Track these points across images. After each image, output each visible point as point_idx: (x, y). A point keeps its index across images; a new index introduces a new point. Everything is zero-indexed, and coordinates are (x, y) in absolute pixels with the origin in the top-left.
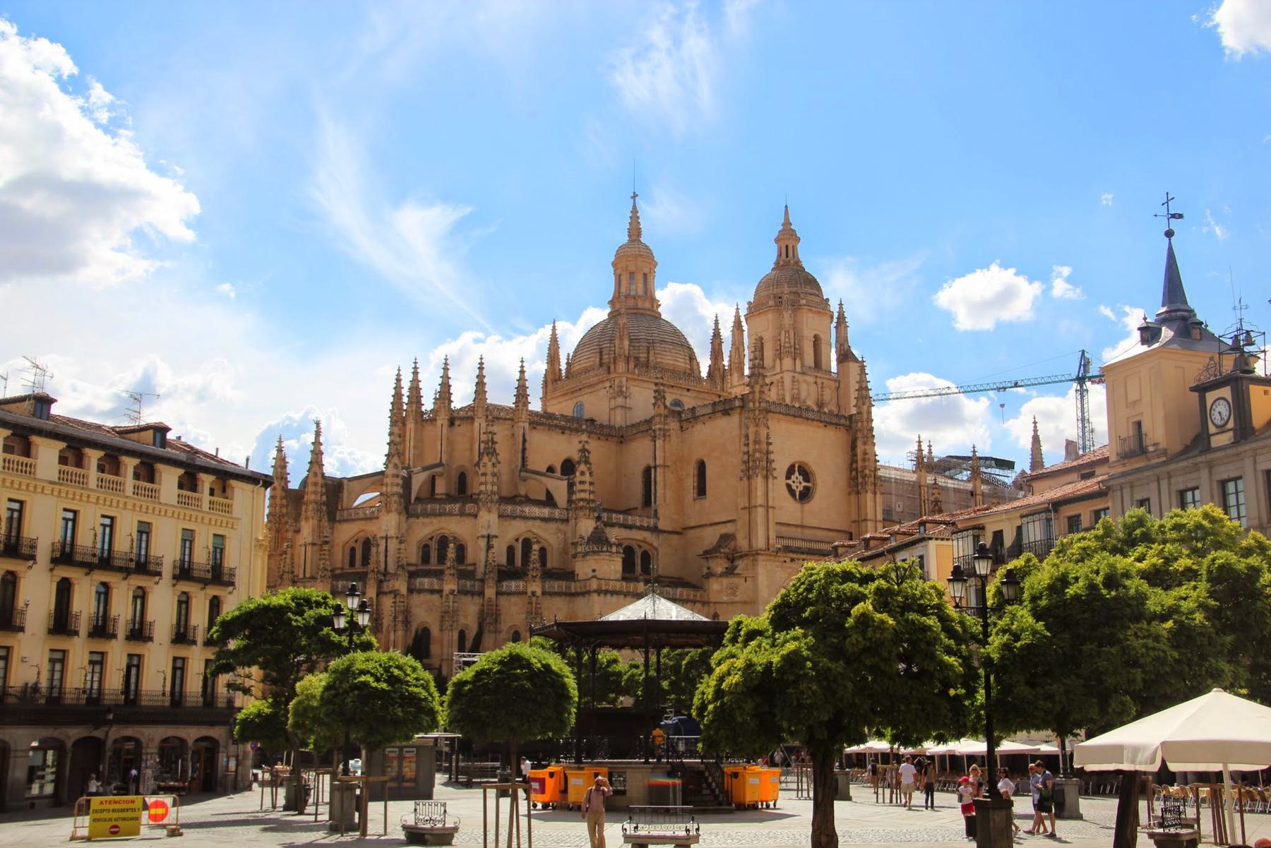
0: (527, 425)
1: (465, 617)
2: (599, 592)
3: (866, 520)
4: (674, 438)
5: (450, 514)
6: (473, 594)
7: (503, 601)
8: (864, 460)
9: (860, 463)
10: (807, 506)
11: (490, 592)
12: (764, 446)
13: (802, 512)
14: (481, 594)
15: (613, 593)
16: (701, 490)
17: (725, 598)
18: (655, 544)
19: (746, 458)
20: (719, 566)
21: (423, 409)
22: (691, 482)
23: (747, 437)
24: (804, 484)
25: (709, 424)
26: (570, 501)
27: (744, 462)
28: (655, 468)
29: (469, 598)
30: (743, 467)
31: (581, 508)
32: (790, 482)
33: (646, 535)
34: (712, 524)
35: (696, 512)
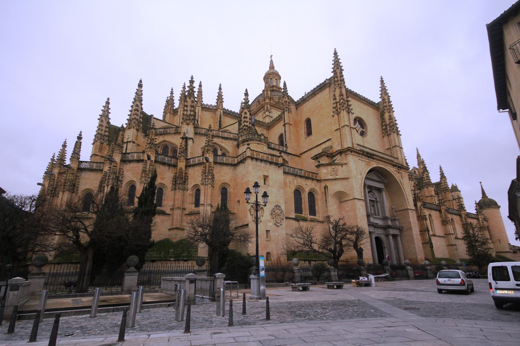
0: (222, 111)
1: (163, 179)
2: (252, 158)
3: (395, 146)
5: (169, 134)
6: (169, 165)
7: (191, 171)
8: (390, 119)
9: (388, 122)
11: (182, 165)
12: (345, 97)
13: (363, 141)
14: (175, 166)
15: (261, 161)
16: (309, 133)
17: (330, 177)
19: (335, 106)
20: (324, 160)
21: (175, 108)
22: (303, 131)
23: (334, 95)
25: (310, 101)
26: (239, 129)
27: (334, 108)
28: (284, 125)
30: (334, 110)
31: (245, 129)
34: (316, 147)
35: (306, 143)
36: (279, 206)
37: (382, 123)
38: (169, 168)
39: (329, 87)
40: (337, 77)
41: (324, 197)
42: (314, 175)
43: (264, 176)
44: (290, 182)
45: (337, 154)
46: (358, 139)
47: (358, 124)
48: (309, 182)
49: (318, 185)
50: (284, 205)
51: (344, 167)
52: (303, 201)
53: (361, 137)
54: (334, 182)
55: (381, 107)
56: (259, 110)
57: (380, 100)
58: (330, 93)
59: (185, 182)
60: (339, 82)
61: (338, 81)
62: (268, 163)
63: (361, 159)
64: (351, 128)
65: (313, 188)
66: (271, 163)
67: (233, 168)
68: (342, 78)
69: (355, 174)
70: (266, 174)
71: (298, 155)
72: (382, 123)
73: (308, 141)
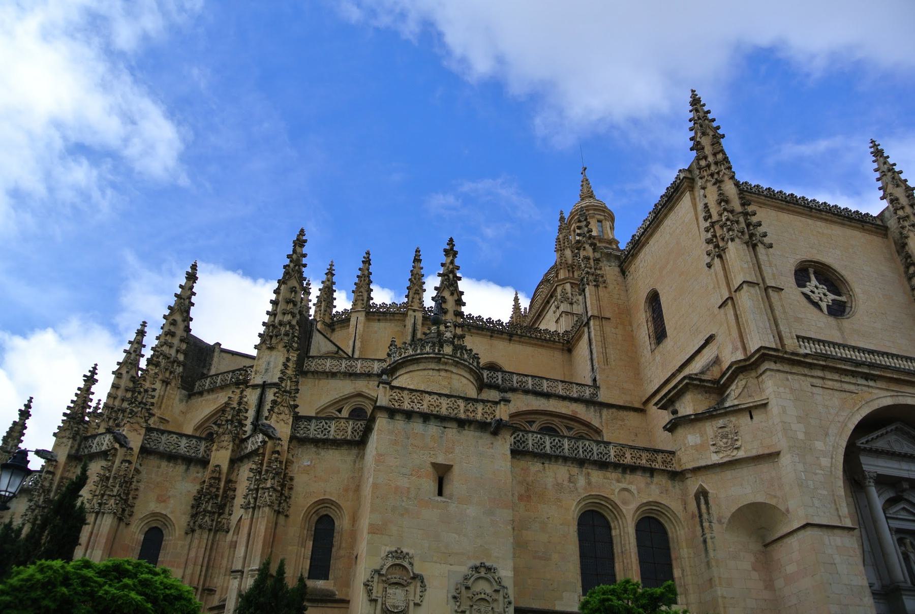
0: (419, 315)
1: (161, 499)
2: (392, 413)
4: (611, 287)
6: (188, 461)
10: (846, 323)
12: (736, 204)
13: (840, 329)
14: (204, 462)
15: (426, 417)
16: (660, 334)
17: (715, 459)
18: (596, 422)
19: (709, 235)
23: (706, 206)
24: (831, 297)
25: (652, 241)
27: (709, 242)
29: (181, 468)
30: (711, 247)
32: (806, 290)
33: (580, 411)
36: (488, 569)
37: (908, 268)
38: (187, 469)
39: (692, 189)
40: (705, 158)
41: (699, 528)
42: (660, 458)
43: (434, 465)
44: (559, 487)
45: (731, 380)
46: (820, 325)
47: (814, 281)
48: (636, 482)
49: (675, 489)
50: (510, 564)
51: (758, 416)
52: (617, 549)
53: (831, 320)
54: (729, 474)
55: (892, 223)
56: (548, 302)
57: (885, 204)
58: (695, 206)
59: (222, 507)
60: (713, 168)
61: (709, 166)
62: (455, 425)
63: (818, 382)
64: (767, 288)
65: (657, 503)
66: (462, 423)
67: (355, 451)
68: (720, 156)
69: (801, 436)
70: (441, 460)
71: (637, 405)
72: (908, 268)
73: (658, 358)
